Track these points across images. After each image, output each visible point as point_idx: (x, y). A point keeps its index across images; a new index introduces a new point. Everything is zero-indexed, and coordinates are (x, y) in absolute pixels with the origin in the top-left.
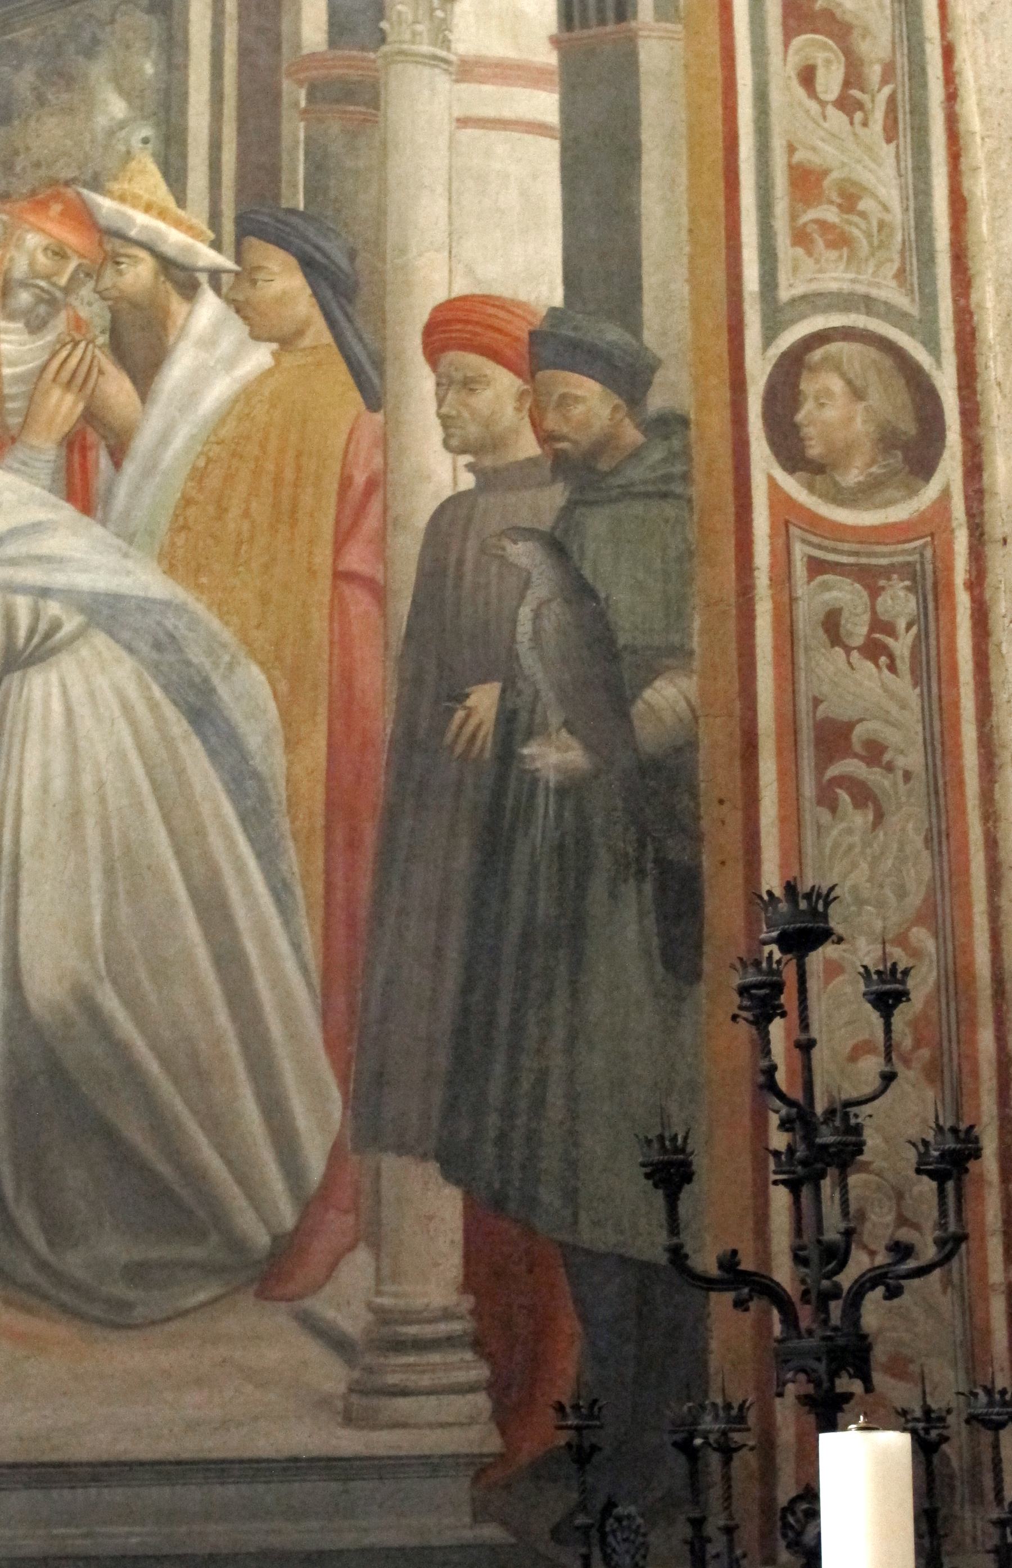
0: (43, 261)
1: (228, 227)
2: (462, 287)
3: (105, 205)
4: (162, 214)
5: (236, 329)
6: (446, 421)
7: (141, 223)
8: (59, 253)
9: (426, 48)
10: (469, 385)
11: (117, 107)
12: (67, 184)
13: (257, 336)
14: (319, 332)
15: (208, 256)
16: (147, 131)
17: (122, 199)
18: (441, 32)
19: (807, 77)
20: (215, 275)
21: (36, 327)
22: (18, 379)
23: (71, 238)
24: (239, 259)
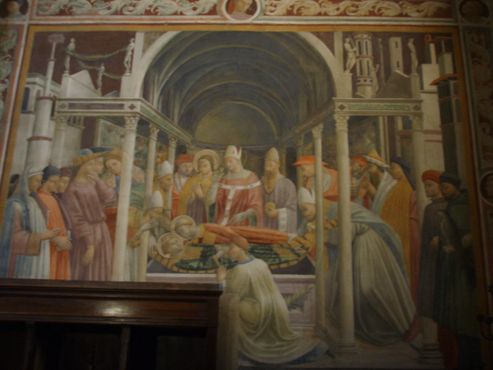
0: (359, 167)
1: (389, 161)
2: (428, 169)
3: (368, 158)
4: (377, 159)
5: (391, 178)
6: (427, 192)
7: (374, 160)
8: (361, 166)
9: (419, 129)
10: (430, 185)
11: (368, 141)
12: (362, 154)
13: (394, 178)
14: (404, 178)
15: (385, 166)
16: (373, 145)
17: (371, 156)
18: (421, 126)
19: (484, 130)
20: (387, 169)
21: (358, 178)
22: (356, 187)
23: (362, 163)
24: (391, 165)
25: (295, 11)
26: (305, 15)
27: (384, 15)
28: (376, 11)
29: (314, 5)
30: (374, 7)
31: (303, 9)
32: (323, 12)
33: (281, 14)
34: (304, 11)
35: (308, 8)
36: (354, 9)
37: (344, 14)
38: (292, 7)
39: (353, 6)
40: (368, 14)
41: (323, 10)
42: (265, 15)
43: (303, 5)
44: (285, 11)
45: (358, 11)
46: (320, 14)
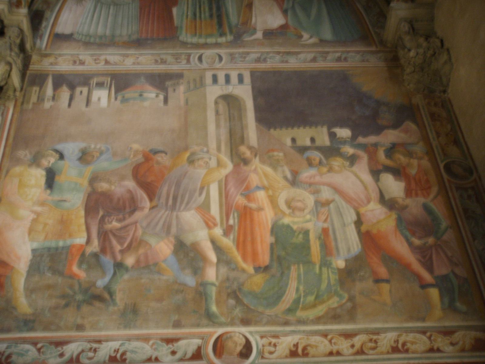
25: (300, 351)
26: (313, 356)
27: (410, 350)
28: (400, 346)
29: (322, 342)
30: (397, 341)
31: (309, 348)
32: (334, 351)
33: (284, 354)
34: (311, 351)
35: (316, 347)
36: (372, 345)
37: (361, 352)
38: (296, 346)
39: (371, 340)
40: (390, 350)
41: (335, 348)
42: (263, 357)
43: (309, 342)
44: (287, 352)
45: (377, 347)
46: (331, 354)
